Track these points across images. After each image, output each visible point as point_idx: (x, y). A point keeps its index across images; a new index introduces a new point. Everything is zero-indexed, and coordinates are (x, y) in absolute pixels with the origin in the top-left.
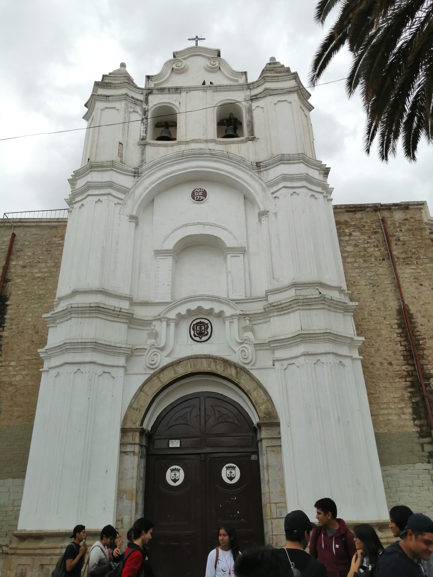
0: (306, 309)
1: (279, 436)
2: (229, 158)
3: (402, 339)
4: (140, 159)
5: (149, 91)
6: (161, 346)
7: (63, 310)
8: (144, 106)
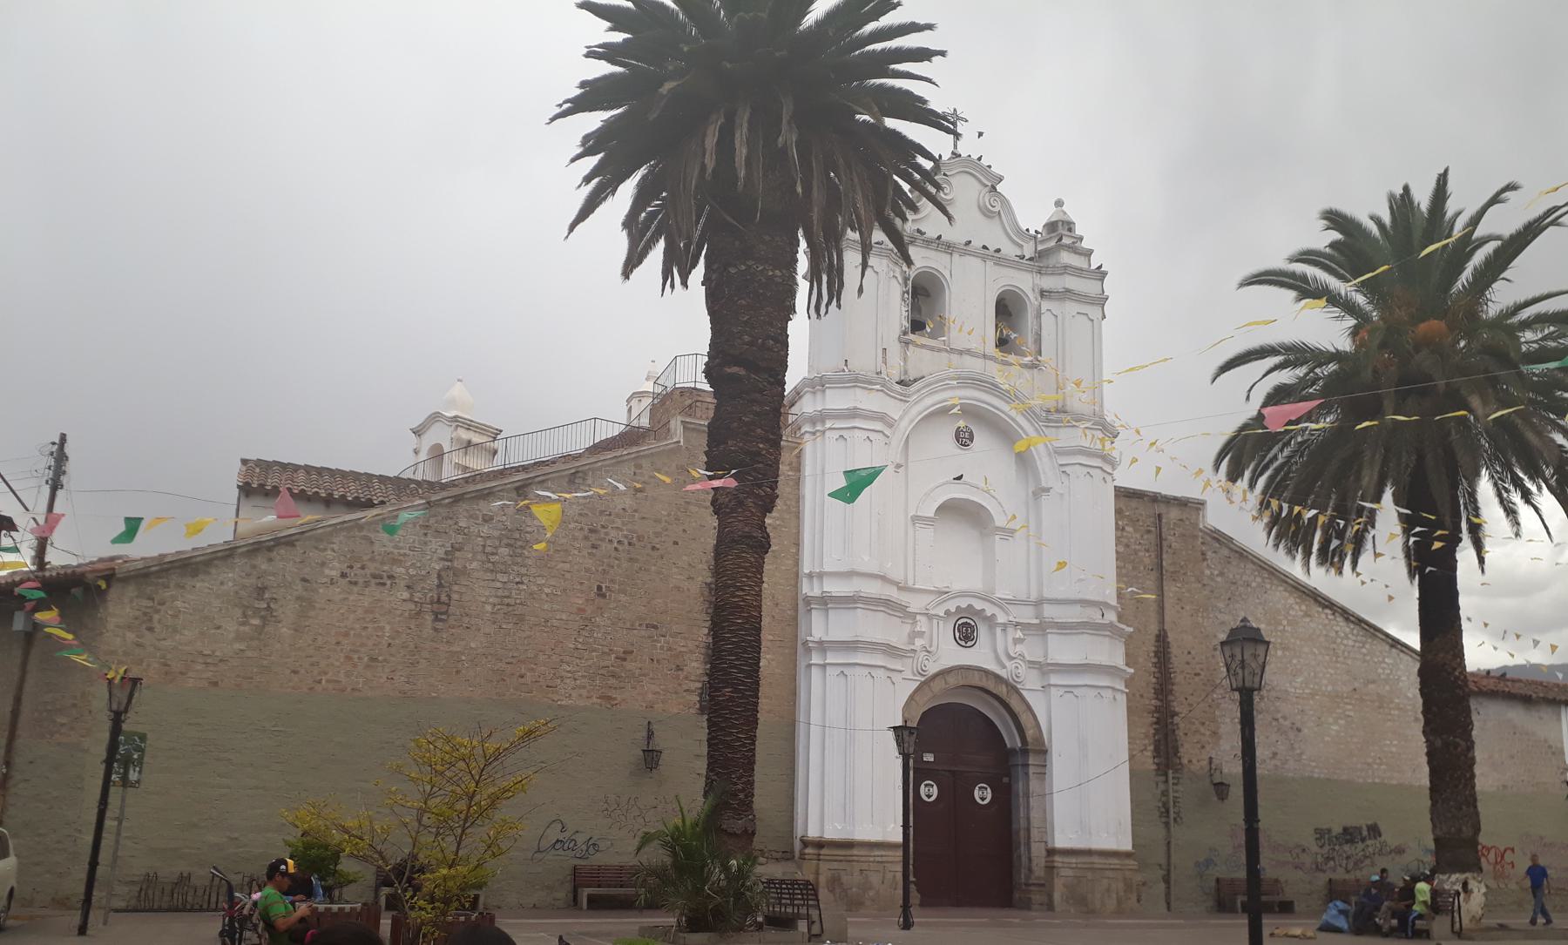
6: (933, 649)
8: (905, 268)
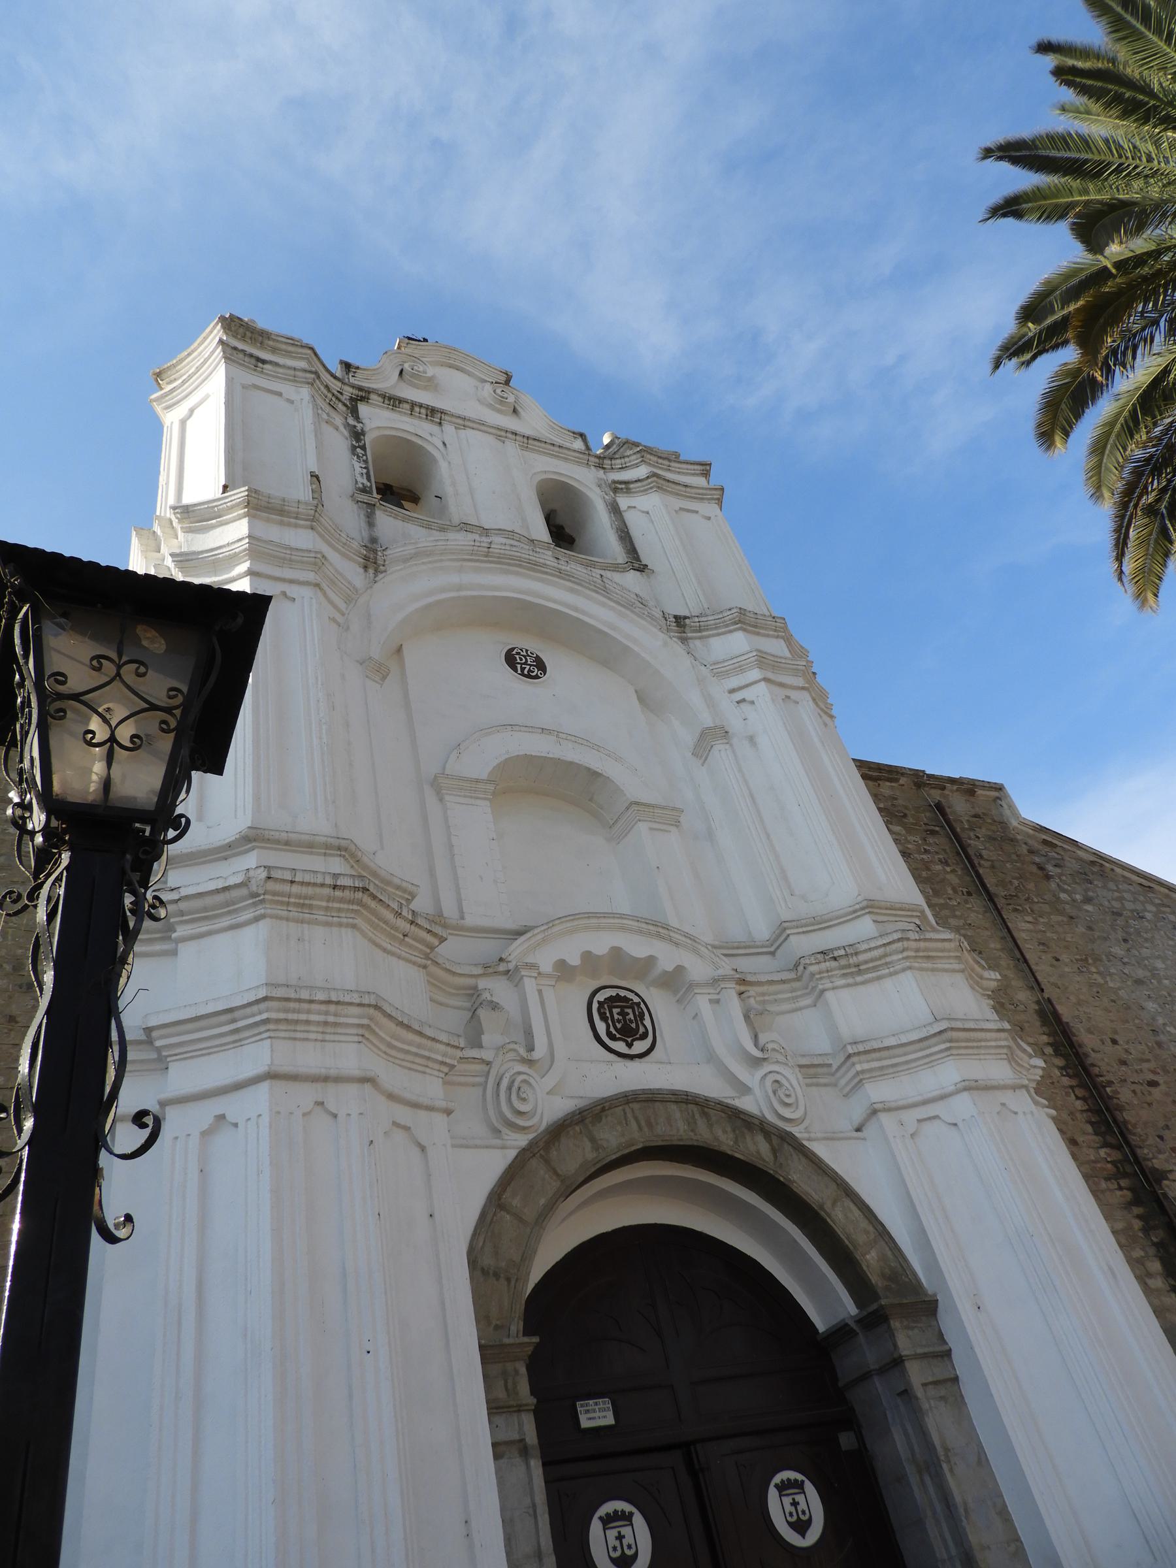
0: (927, 970)
1: (946, 1348)
2: (605, 589)
3: (1074, 1083)
4: (365, 534)
5: (360, 393)
6: (536, 1055)
7: (226, 889)
8: (351, 421)
